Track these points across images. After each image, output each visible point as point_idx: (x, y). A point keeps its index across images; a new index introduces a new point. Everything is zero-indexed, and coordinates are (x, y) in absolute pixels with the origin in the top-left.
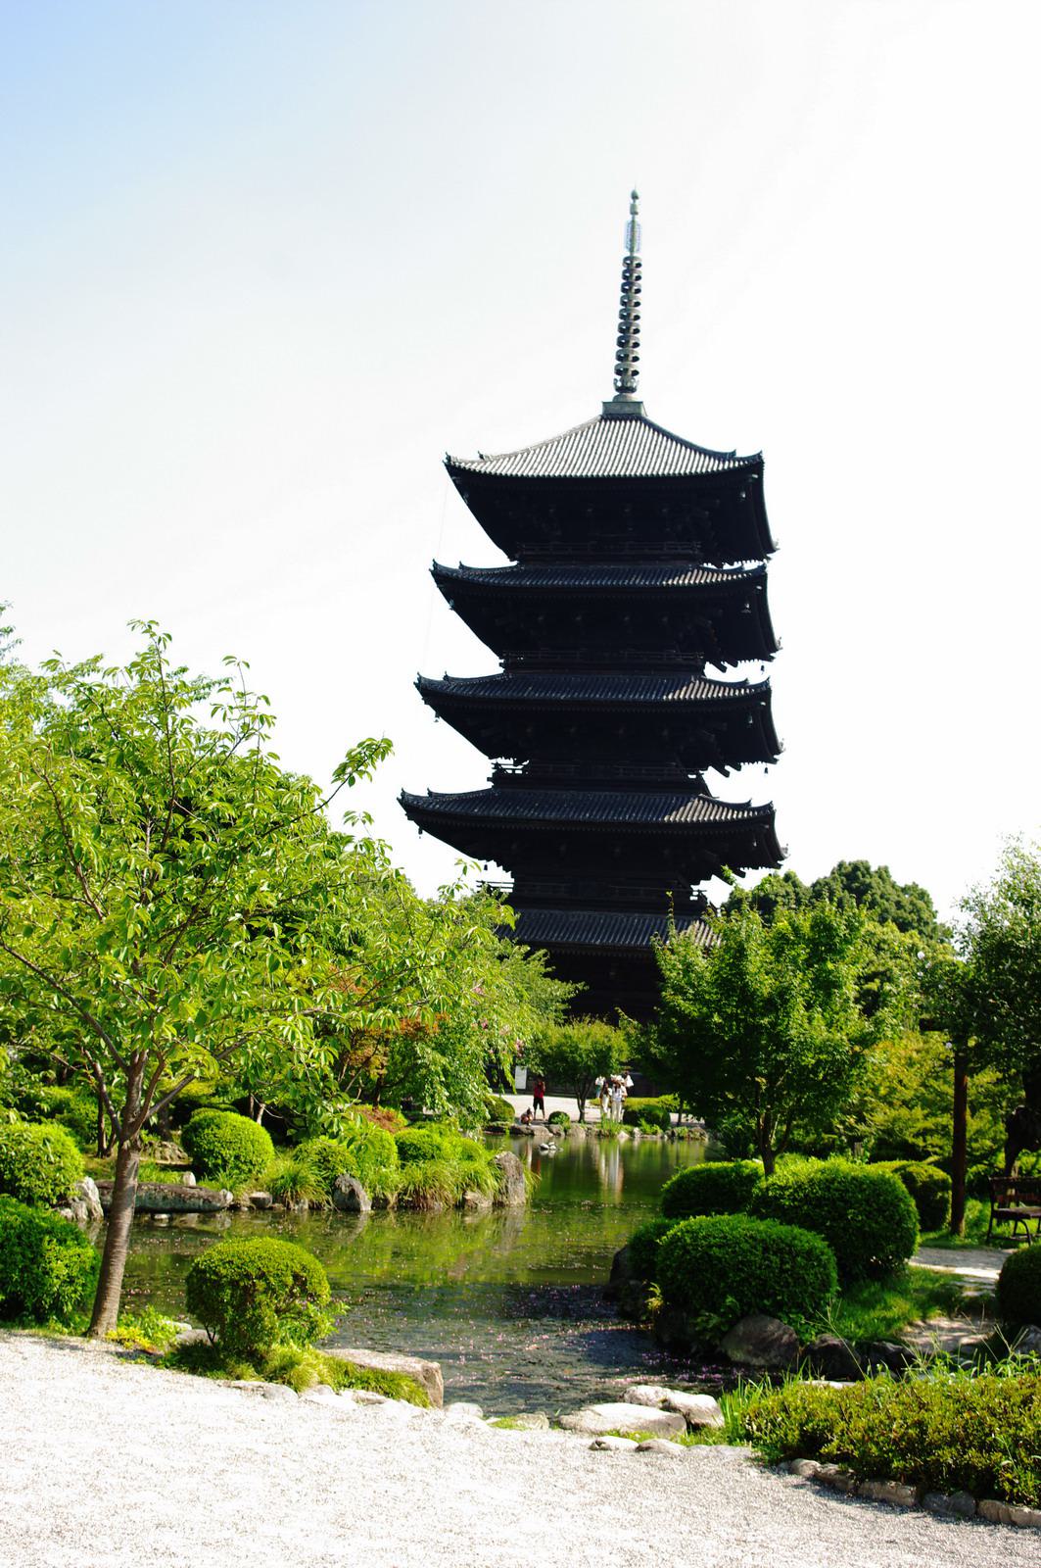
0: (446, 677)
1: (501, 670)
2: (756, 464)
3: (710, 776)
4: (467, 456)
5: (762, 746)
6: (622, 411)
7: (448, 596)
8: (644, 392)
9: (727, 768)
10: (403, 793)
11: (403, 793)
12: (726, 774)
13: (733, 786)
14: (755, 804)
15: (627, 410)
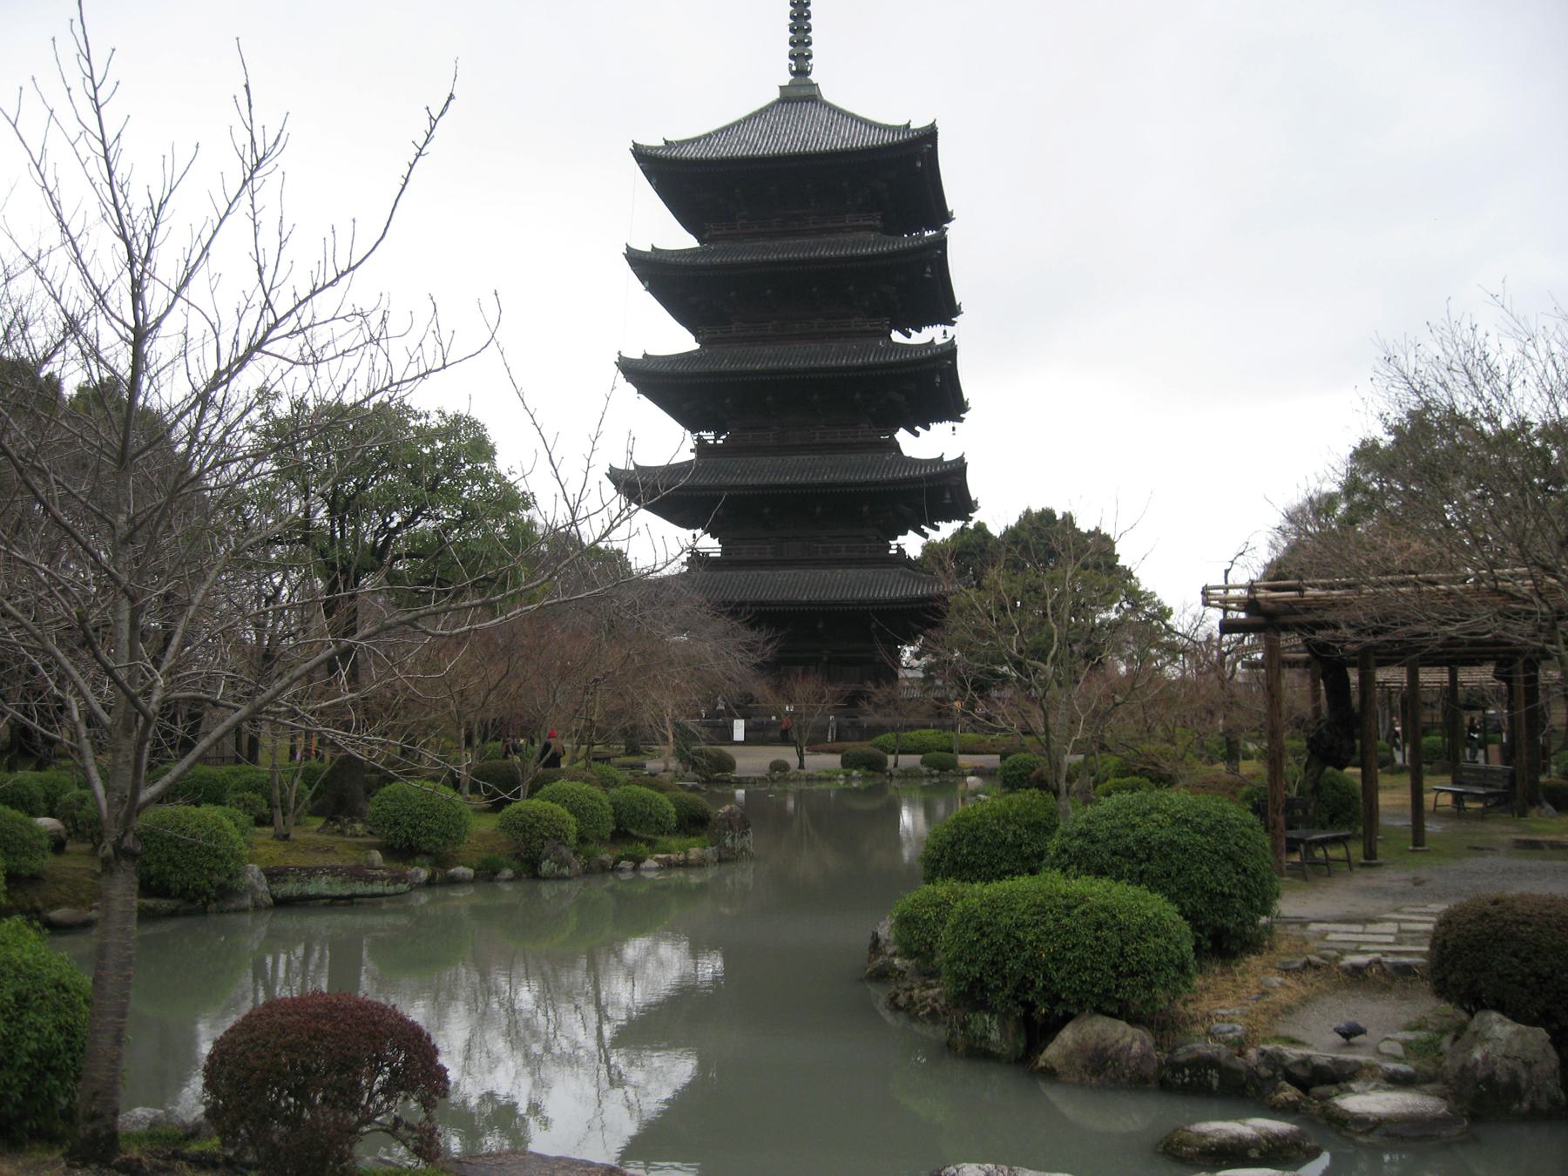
0: (645, 355)
1: (697, 346)
2: (930, 135)
3: (902, 436)
4: (653, 139)
5: (950, 405)
6: (800, 93)
7: (642, 278)
8: (819, 74)
9: (918, 428)
10: (611, 468)
11: (611, 468)
12: (917, 434)
13: (922, 444)
14: (946, 459)
15: (804, 92)
